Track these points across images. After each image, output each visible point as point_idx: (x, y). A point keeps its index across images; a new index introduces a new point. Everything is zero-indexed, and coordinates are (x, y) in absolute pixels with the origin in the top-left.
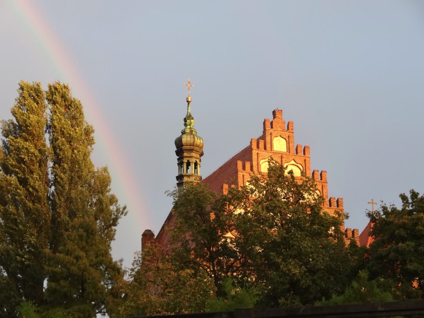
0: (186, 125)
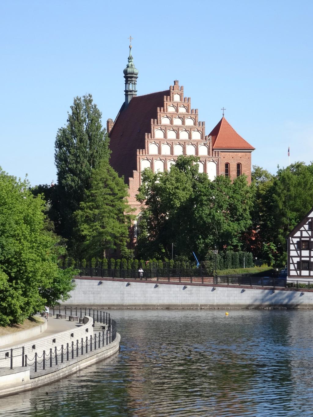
0: (129, 62)
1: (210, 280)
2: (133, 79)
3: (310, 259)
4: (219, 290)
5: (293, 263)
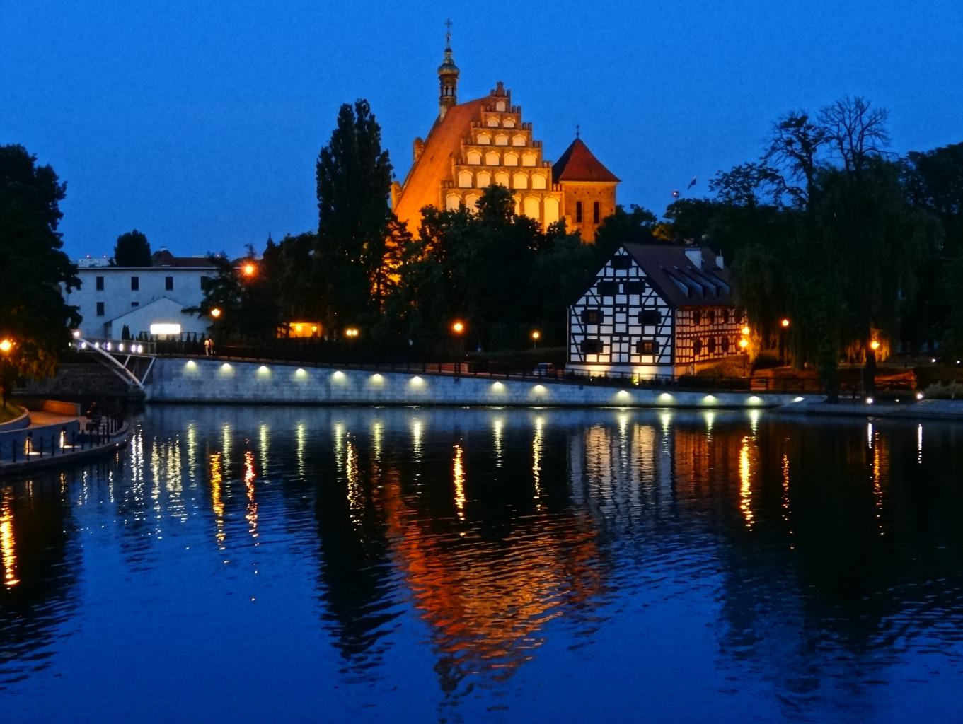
1: (449, 368)
3: (599, 338)
4: (464, 380)
5: (576, 344)
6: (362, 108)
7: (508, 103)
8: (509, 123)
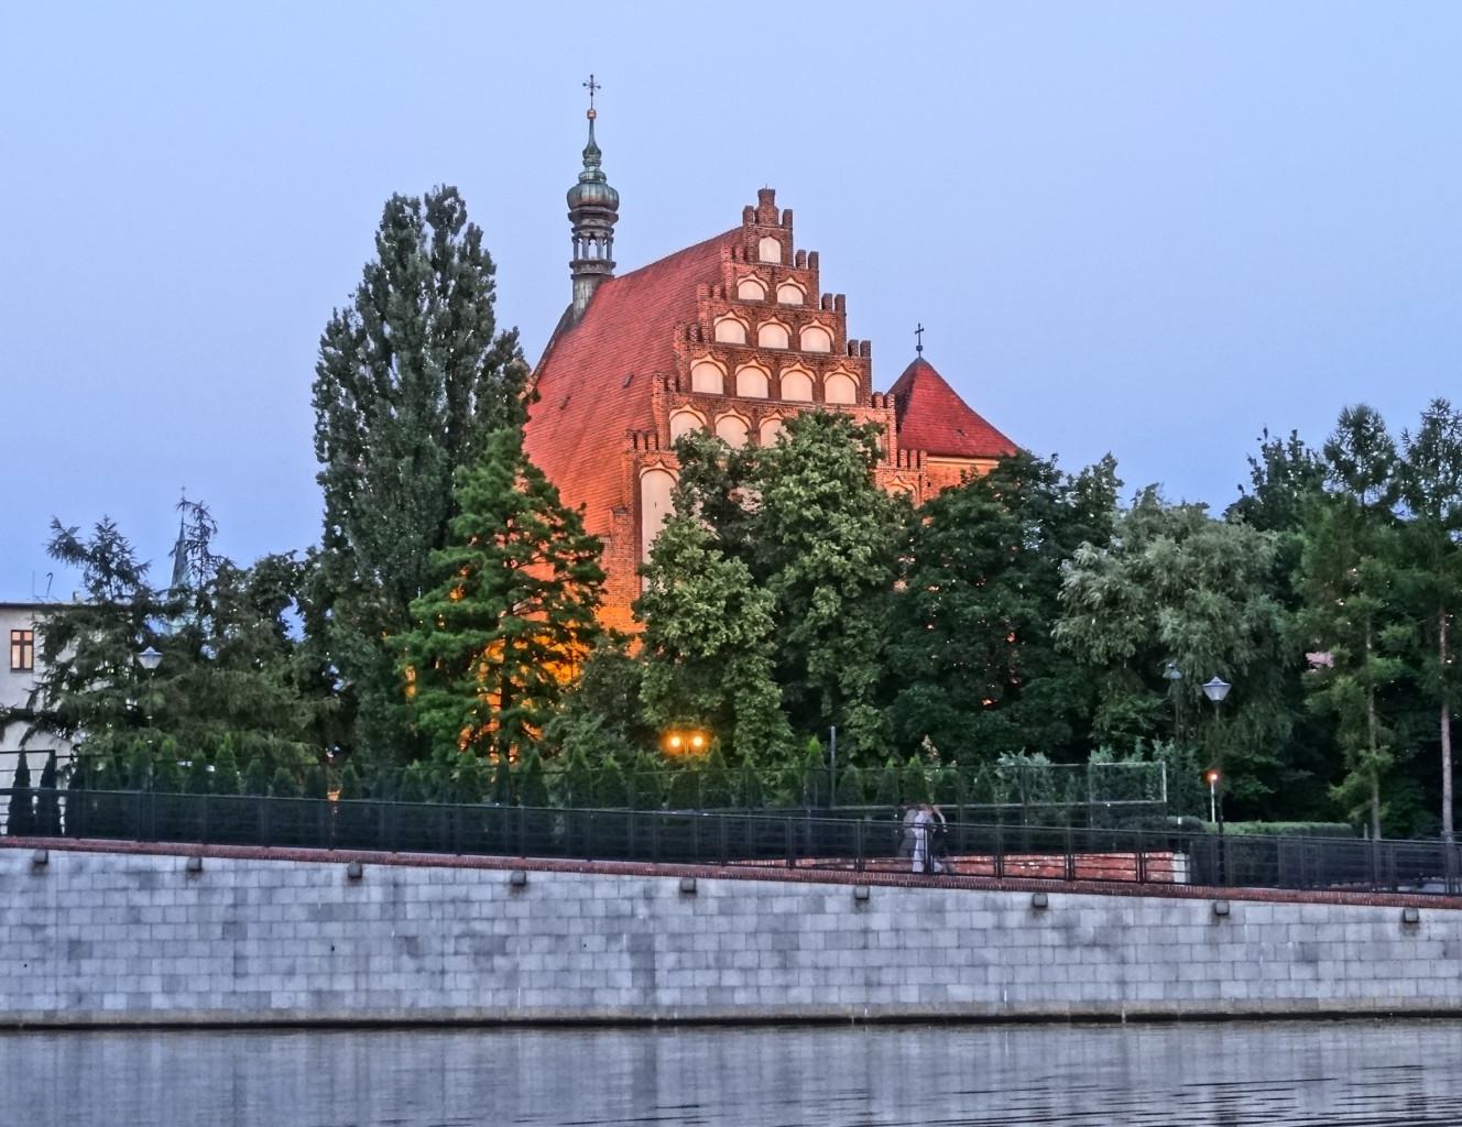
2: (601, 222)
6: (445, 211)
7: (786, 240)
8: (789, 295)
